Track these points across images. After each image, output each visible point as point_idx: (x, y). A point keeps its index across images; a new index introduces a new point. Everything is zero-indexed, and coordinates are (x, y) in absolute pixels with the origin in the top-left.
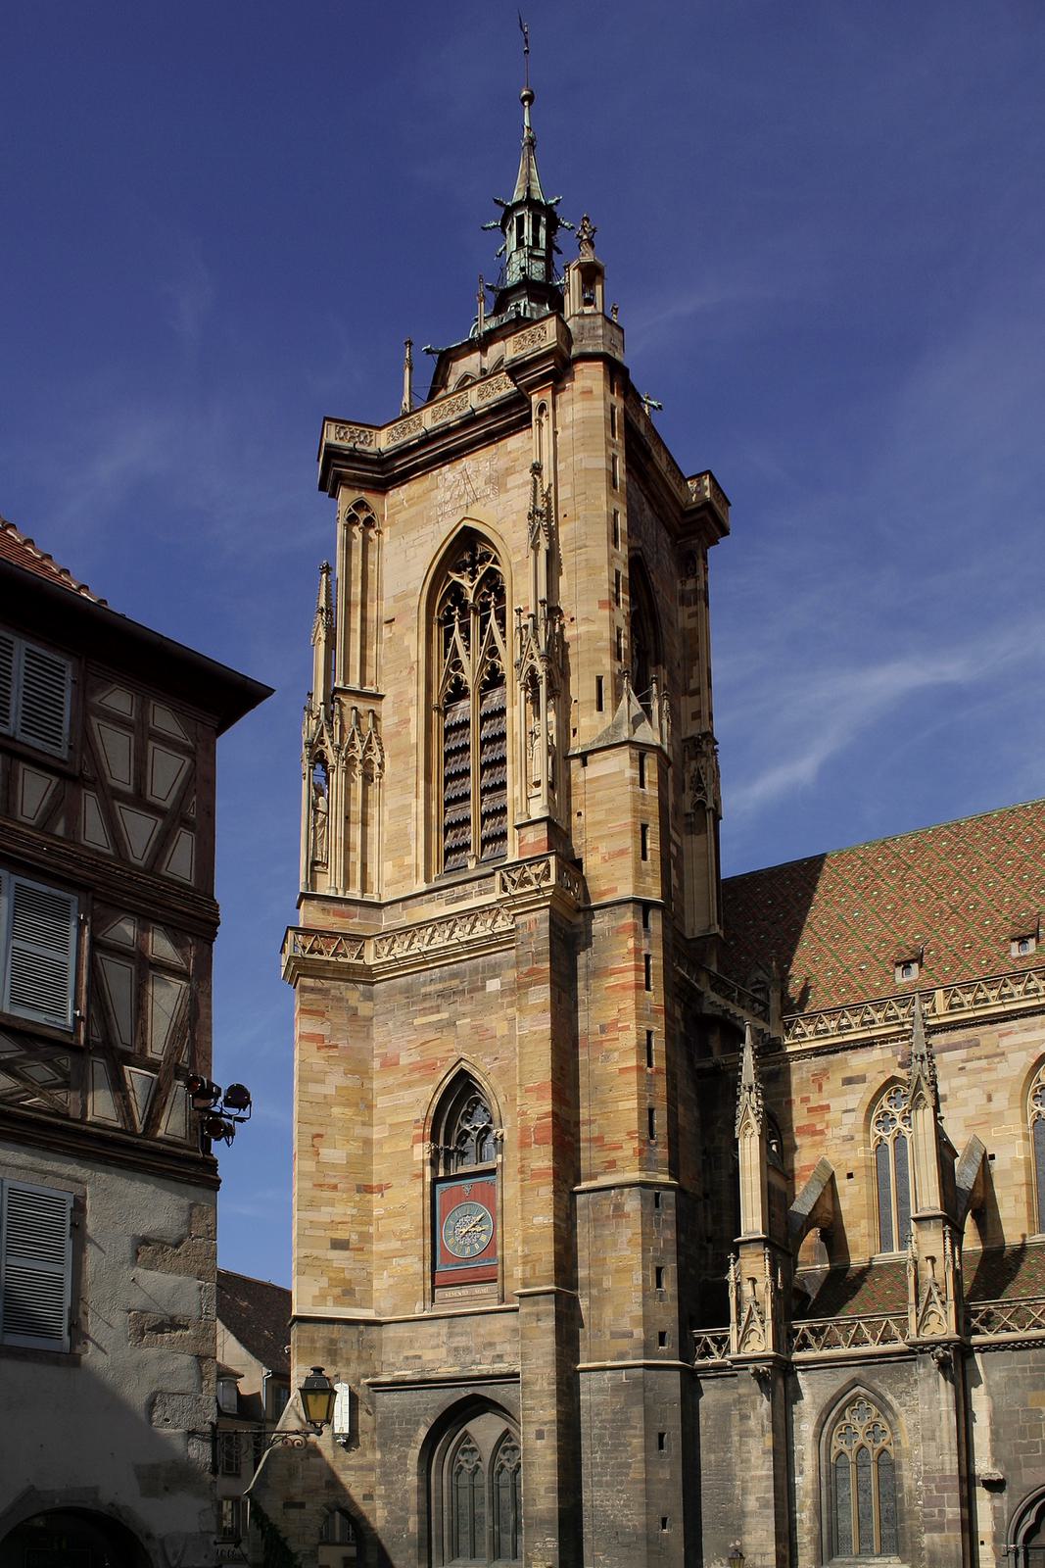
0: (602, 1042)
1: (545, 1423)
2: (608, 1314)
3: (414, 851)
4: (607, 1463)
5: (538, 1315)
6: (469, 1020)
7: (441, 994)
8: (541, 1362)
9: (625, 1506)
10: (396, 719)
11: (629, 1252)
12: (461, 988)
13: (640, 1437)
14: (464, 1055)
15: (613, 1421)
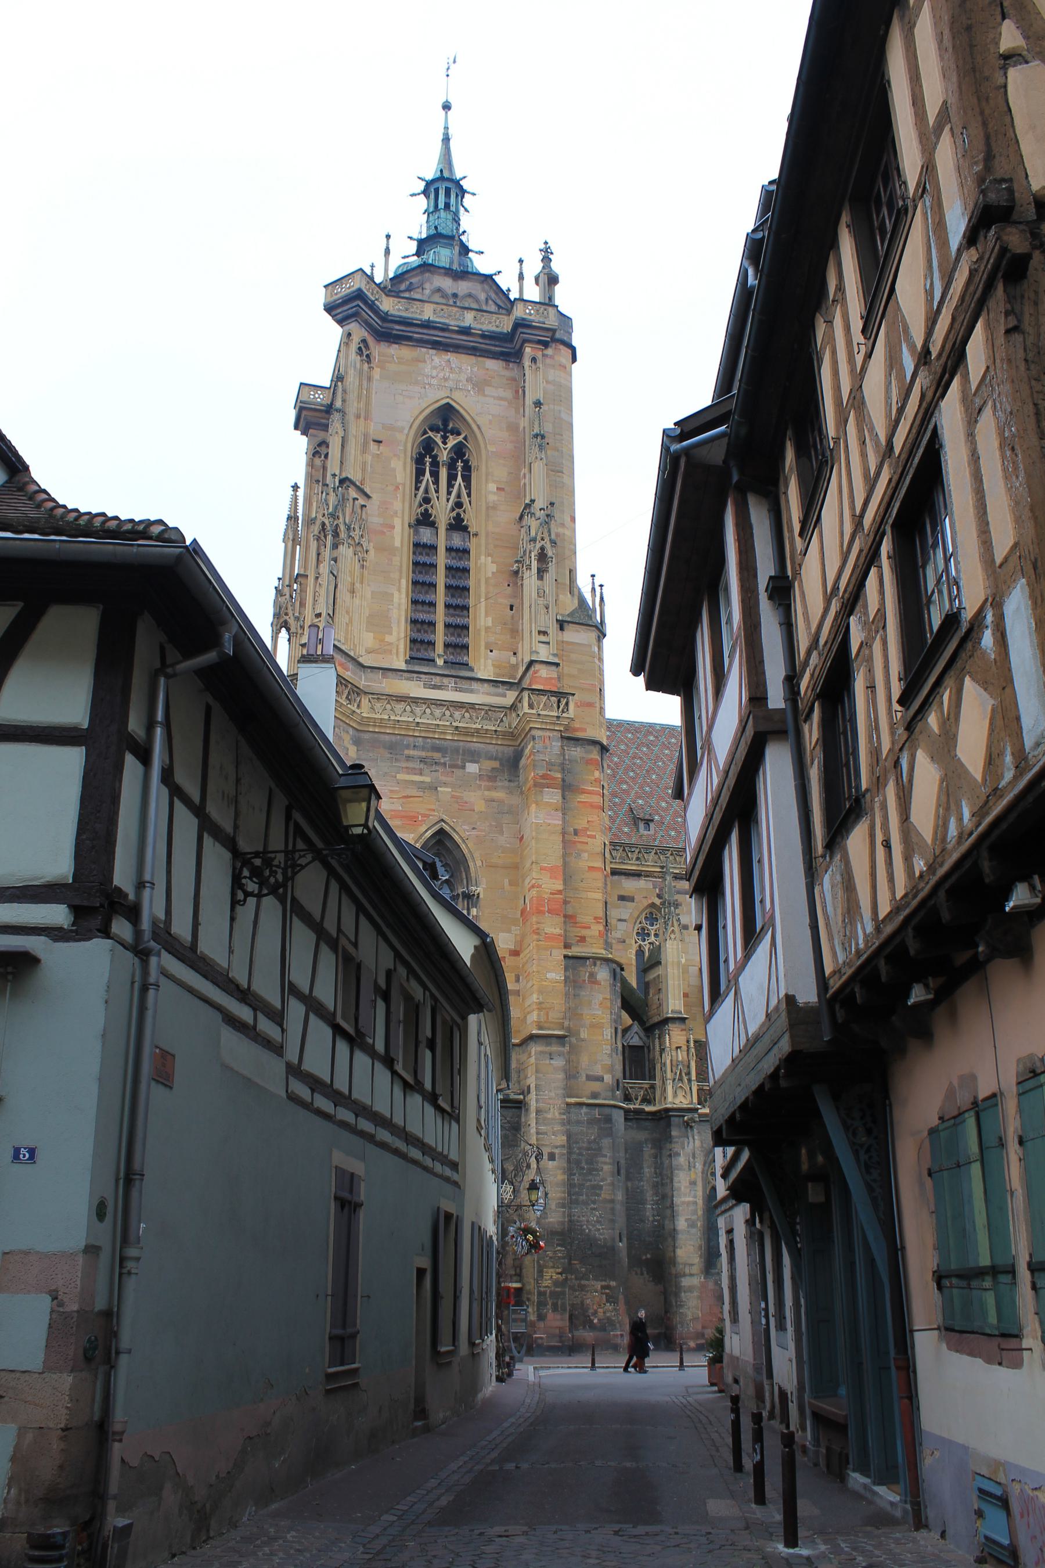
0: (575, 842)
1: (557, 1147)
2: (584, 1060)
3: (395, 633)
4: (583, 1185)
5: (550, 1054)
6: (450, 790)
7: (422, 760)
8: (553, 1094)
9: (598, 1222)
10: (381, 521)
11: (600, 1013)
12: (442, 761)
13: (610, 1164)
14: (445, 817)
15: (588, 1149)
